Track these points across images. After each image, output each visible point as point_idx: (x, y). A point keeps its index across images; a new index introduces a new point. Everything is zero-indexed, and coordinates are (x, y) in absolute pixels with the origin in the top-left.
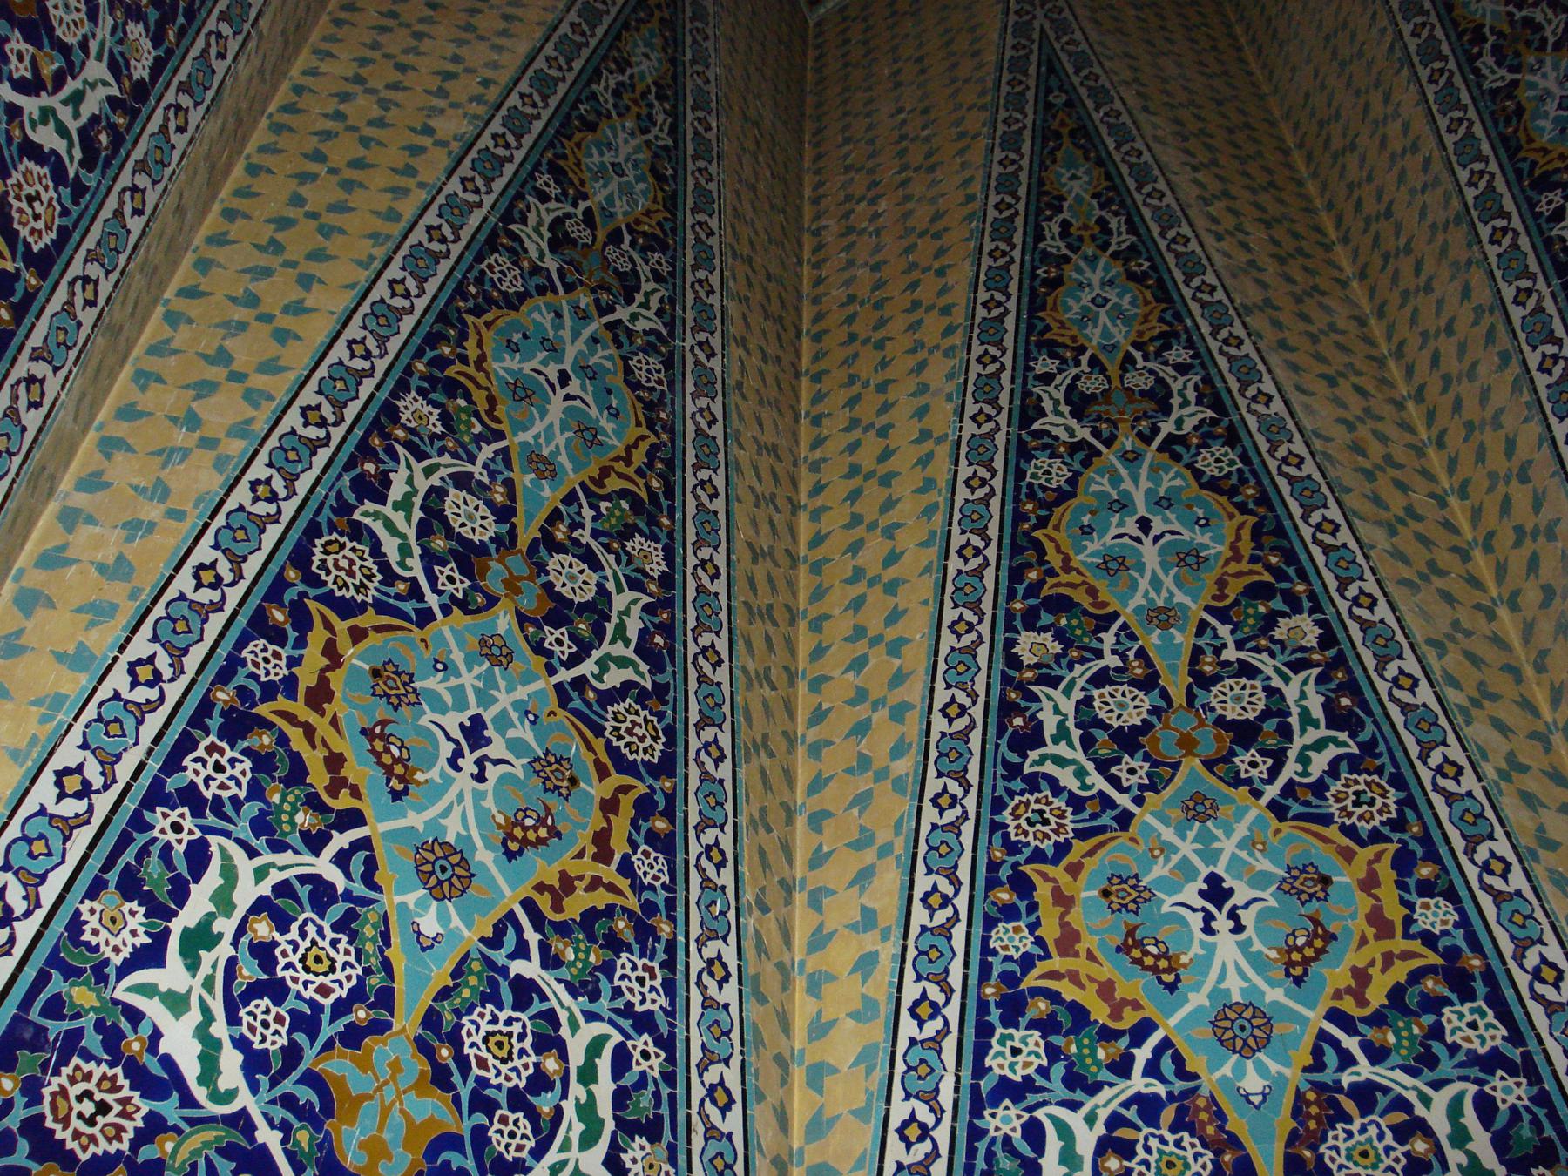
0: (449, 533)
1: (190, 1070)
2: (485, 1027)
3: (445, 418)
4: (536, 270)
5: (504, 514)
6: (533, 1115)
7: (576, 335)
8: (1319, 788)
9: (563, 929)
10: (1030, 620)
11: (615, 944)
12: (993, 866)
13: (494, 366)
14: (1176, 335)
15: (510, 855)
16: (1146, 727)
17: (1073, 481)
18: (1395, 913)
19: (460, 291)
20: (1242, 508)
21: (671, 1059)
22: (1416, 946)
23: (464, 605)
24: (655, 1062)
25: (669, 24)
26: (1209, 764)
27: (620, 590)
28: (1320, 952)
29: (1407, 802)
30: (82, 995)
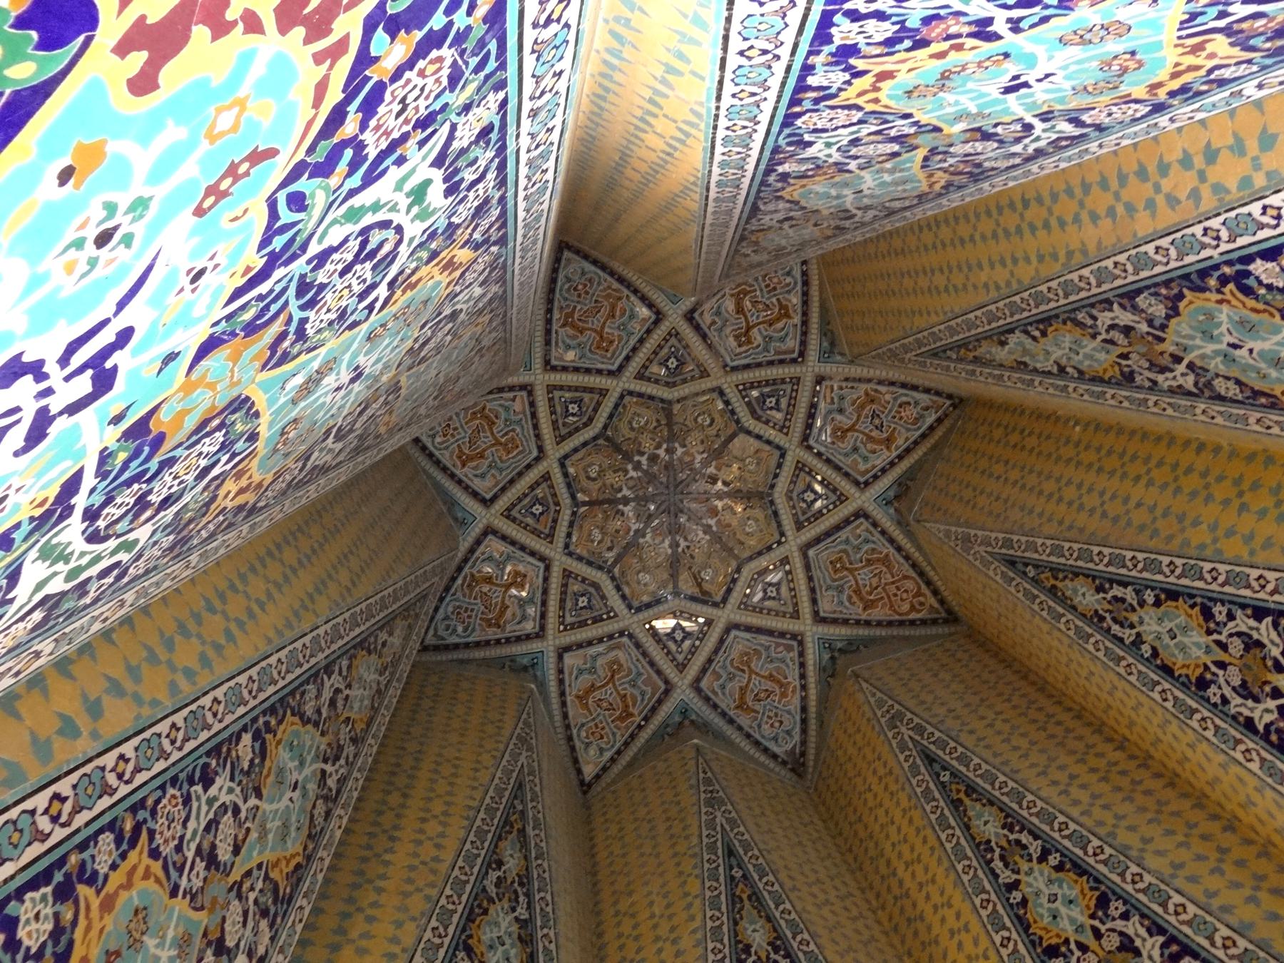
17: (309, 721)
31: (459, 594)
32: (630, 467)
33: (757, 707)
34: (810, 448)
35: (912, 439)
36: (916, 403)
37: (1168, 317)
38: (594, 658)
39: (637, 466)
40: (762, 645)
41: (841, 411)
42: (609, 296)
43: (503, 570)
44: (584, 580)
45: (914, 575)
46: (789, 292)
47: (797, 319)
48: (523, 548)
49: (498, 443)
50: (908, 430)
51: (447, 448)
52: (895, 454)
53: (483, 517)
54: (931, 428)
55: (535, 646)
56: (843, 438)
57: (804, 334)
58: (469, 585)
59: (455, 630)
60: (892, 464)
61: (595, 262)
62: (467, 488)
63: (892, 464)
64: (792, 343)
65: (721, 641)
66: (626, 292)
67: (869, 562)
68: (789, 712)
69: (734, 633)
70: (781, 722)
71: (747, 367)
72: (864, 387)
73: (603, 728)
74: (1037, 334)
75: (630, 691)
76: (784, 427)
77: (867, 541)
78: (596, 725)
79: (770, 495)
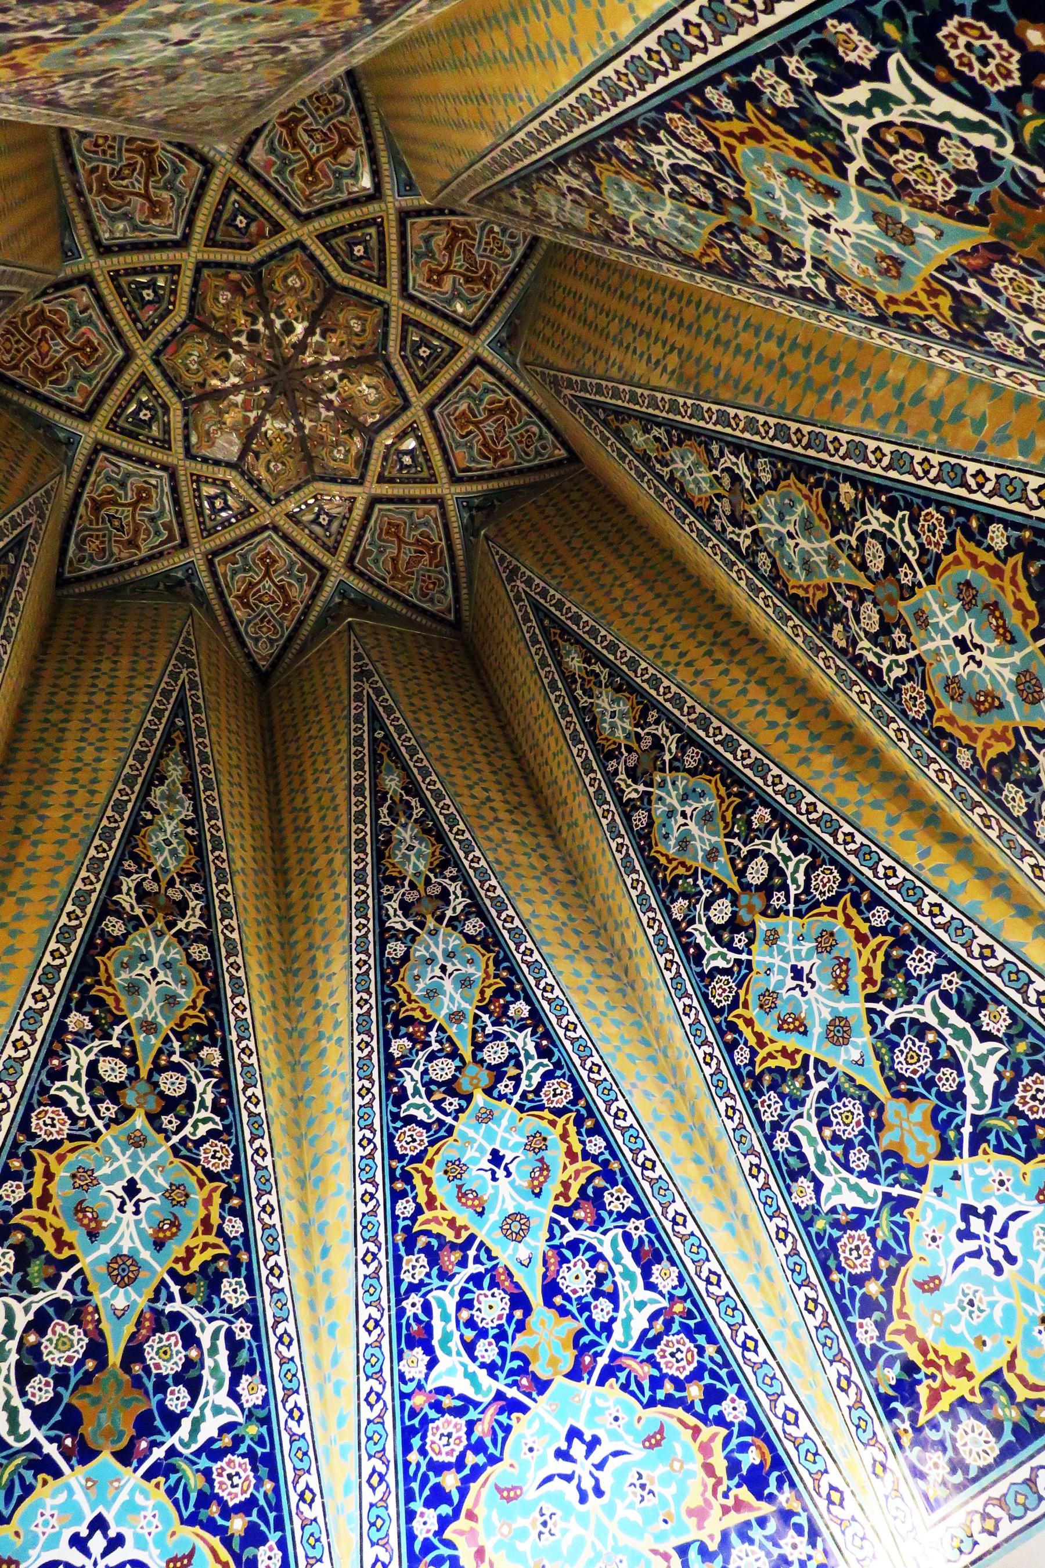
0: (722, 927)
1: (860, 1203)
2: (902, 1059)
3: (685, 895)
4: (641, 799)
5: (725, 892)
6: (945, 1063)
7: (669, 794)
8: (924, 551)
9: (885, 987)
10: (830, 630)
11: (901, 962)
12: (930, 737)
13: (671, 852)
14: (706, 444)
15: (846, 993)
16: (880, 612)
18: (990, 559)
19: (642, 850)
20: (787, 477)
21: (958, 969)
22: (1011, 561)
23: (751, 941)
24: (955, 979)
25: (565, 631)
26: (903, 599)
27: (768, 846)
28: (1002, 617)
29: (939, 505)
30: (820, 1224)
31: (501, 269)
32: (336, 404)
33: (125, 155)
34: (164, 468)
35: (77, 521)
36: (92, 561)
37: (188, 955)
38: (338, 189)
39: (329, 404)
40: (143, 230)
41: (153, 519)
42: (404, 579)
43: (454, 288)
44: (361, 275)
45: (9, 373)
46: (249, 622)
47: (230, 600)
48: (434, 310)
49: (476, 424)
50: (85, 529)
51: (527, 423)
52: (85, 497)
53: (481, 345)
54: (65, 541)
55: (410, 202)
56: (140, 491)
57: (217, 584)
58: (490, 276)
59: (504, 231)
60: (82, 484)
61: (424, 612)
62: (500, 378)
63: (82, 484)
64: (220, 570)
65: (190, 223)
66: (388, 585)
67: (58, 367)
68: (90, 160)
69: (178, 236)
70: (96, 145)
71: (254, 533)
72: (144, 553)
73: (318, 109)
74: (189, 830)
75: (289, 153)
76: (198, 481)
77: (70, 389)
78: (326, 111)
79: (184, 404)
